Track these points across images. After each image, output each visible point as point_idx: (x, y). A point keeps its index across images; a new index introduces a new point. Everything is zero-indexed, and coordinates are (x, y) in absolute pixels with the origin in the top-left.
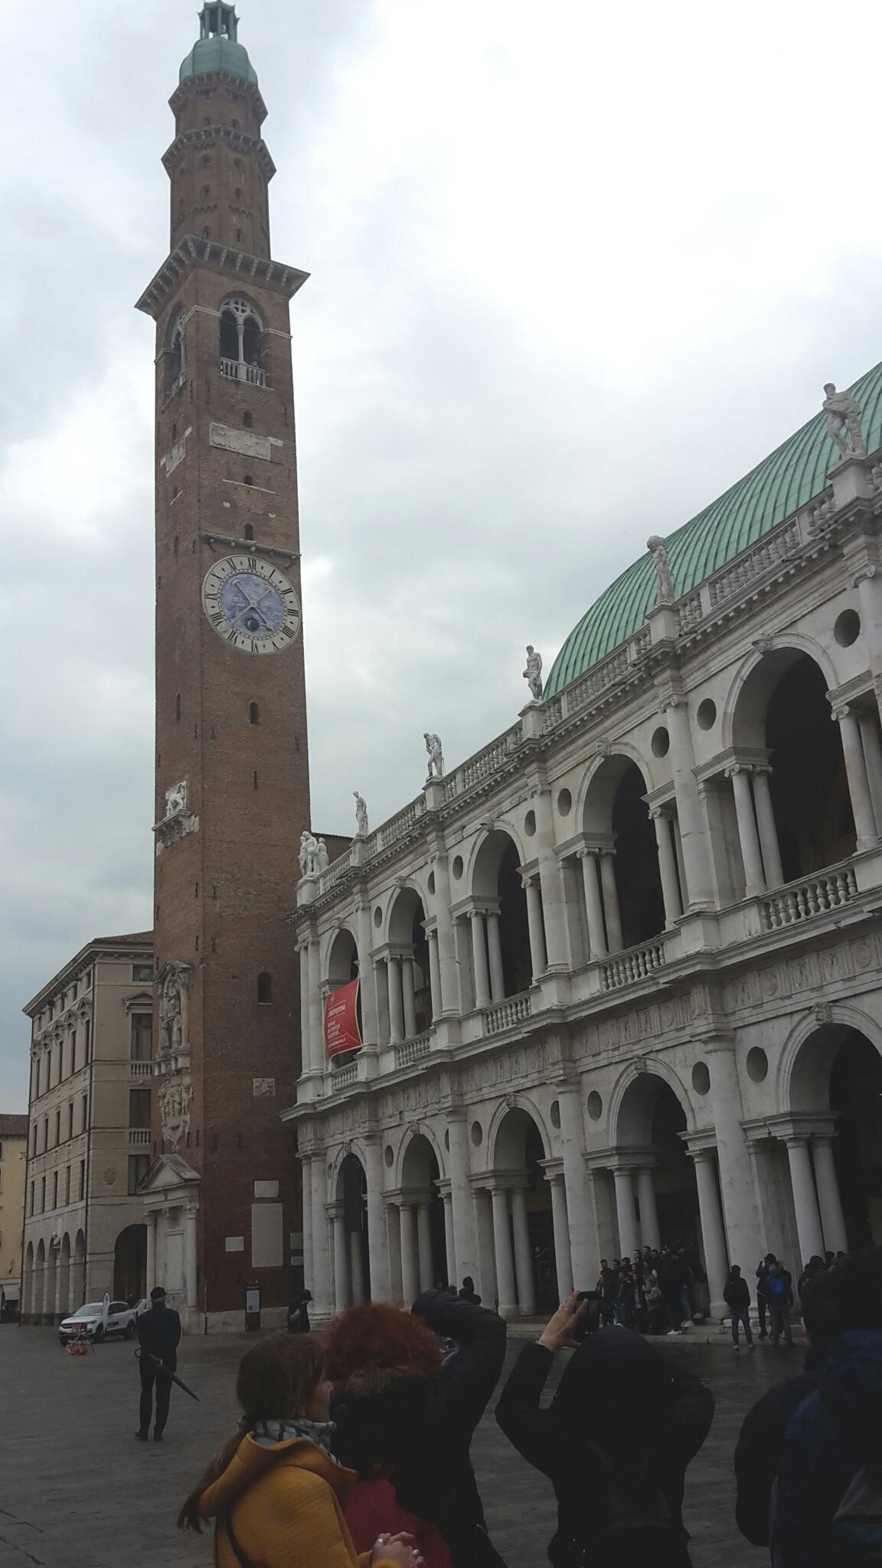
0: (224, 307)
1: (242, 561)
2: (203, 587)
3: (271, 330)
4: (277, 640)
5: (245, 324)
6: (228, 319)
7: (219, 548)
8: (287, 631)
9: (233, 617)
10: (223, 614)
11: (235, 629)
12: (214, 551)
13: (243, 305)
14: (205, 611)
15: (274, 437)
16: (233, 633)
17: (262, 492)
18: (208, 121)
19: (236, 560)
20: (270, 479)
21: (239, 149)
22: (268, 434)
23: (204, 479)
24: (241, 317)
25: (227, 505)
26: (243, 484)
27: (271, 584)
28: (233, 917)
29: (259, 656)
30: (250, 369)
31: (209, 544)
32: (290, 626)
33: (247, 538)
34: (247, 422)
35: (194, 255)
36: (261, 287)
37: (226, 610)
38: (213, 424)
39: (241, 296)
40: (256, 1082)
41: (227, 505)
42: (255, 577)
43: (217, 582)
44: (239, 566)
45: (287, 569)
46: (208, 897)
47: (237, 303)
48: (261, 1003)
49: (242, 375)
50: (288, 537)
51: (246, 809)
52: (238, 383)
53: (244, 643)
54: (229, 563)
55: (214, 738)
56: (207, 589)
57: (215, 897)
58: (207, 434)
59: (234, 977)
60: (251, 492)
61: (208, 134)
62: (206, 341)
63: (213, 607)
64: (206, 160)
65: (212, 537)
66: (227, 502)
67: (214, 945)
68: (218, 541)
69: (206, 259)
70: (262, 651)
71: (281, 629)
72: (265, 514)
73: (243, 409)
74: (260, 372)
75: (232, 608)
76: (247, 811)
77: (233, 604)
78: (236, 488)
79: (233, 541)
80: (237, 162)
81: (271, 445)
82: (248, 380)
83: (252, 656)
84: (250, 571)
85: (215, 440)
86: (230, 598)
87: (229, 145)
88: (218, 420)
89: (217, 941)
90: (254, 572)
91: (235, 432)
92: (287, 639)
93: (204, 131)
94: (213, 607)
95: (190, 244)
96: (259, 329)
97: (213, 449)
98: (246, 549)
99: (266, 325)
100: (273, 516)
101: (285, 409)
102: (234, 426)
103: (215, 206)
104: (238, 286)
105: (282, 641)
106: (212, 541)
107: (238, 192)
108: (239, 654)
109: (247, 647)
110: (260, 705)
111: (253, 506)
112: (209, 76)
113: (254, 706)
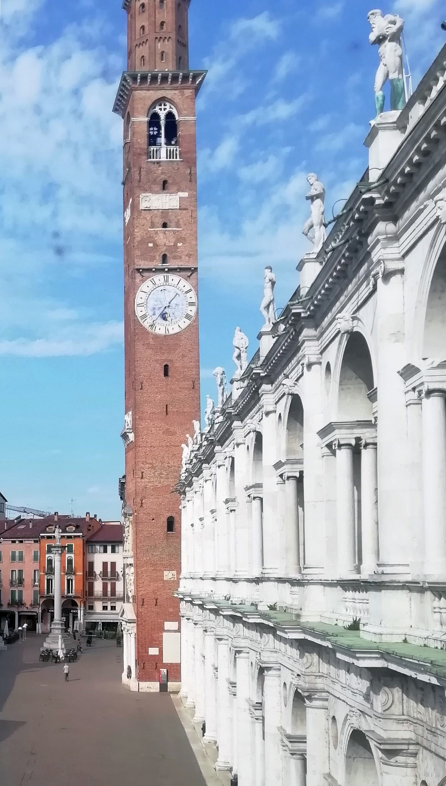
0: (152, 111)
1: (159, 278)
2: (135, 300)
7: (146, 274)
10: (147, 314)
13: (165, 105)
14: (137, 314)
15: (183, 191)
17: (174, 231)
22: (179, 190)
23: (137, 232)
24: (162, 115)
29: (171, 335)
30: (169, 149)
32: (190, 313)
34: (165, 185)
35: (131, 84)
36: (176, 90)
39: (161, 100)
40: (165, 573)
41: (151, 245)
43: (144, 295)
44: (157, 282)
45: (189, 277)
46: (138, 478)
47: (161, 105)
48: (168, 533)
51: (160, 427)
53: (161, 329)
54: (152, 282)
56: (138, 301)
57: (142, 478)
58: (139, 203)
59: (153, 519)
60: (166, 232)
65: (140, 269)
67: (142, 503)
70: (172, 332)
73: (162, 179)
76: (161, 428)
78: (156, 233)
82: (167, 158)
83: (165, 336)
84: (165, 284)
86: (151, 303)
88: (146, 191)
89: (143, 501)
96: (175, 118)
97: (143, 211)
99: (180, 114)
101: (190, 170)
102: (157, 193)
103: (147, 40)
104: (160, 94)
106: (141, 270)
108: (156, 337)
109: (162, 332)
110: (169, 365)
113: (166, 367)
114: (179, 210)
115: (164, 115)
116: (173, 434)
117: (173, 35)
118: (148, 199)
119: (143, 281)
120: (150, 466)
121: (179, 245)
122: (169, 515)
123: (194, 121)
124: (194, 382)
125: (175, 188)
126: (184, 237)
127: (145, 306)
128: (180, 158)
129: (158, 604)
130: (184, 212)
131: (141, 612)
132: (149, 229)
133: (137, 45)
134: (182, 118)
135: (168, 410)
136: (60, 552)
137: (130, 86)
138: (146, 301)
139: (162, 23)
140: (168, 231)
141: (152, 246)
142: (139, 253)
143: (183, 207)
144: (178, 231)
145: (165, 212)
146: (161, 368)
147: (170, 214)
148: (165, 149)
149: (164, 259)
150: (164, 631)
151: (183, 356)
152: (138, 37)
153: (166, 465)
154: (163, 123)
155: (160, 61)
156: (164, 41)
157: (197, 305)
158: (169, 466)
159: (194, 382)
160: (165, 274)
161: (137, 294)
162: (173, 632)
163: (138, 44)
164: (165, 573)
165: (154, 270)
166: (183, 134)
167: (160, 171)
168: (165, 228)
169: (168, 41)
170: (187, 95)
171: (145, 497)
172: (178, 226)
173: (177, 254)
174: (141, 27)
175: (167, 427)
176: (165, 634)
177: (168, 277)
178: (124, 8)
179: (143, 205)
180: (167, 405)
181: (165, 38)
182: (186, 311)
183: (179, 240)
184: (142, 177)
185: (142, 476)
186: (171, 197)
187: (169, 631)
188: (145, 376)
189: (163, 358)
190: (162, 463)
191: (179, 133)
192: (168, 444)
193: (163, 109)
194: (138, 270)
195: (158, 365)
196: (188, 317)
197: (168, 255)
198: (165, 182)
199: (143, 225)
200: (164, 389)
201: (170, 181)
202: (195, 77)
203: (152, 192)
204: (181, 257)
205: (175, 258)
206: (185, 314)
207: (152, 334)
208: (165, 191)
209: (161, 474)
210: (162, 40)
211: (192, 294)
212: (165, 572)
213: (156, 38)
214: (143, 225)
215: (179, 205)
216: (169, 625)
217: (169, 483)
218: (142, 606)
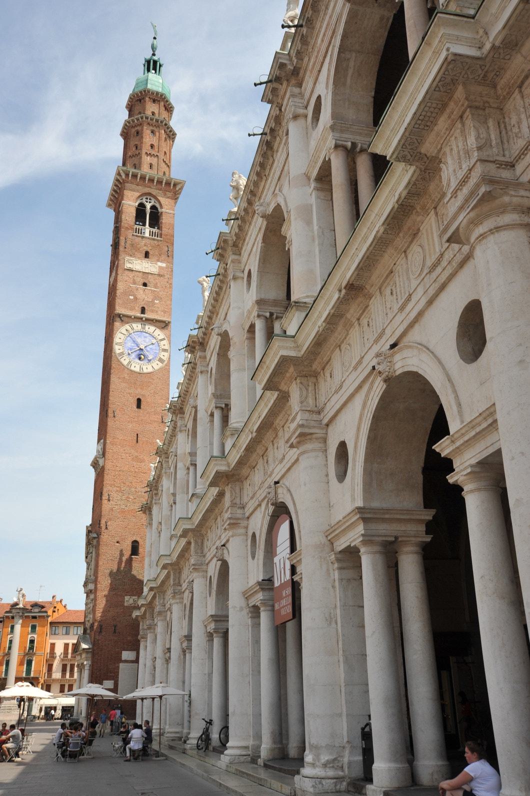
1: (137, 326)
3: (163, 210)
4: (154, 365)
5: (150, 209)
6: (142, 205)
12: (122, 321)
13: (150, 199)
15: (161, 262)
16: (130, 362)
19: (134, 325)
21: (154, 125)
22: (158, 261)
24: (148, 206)
25: (132, 297)
26: (142, 287)
27: (153, 337)
30: (151, 231)
31: (120, 317)
34: (147, 255)
36: (160, 190)
38: (127, 258)
40: (127, 598)
41: (132, 297)
42: (145, 334)
47: (147, 199)
50: (165, 312)
53: (136, 366)
61: (138, 120)
63: (119, 349)
66: (132, 296)
69: (130, 178)
70: (145, 371)
72: (153, 301)
74: (157, 232)
79: (133, 315)
82: (150, 235)
84: (142, 330)
85: (128, 265)
87: (149, 124)
90: (144, 331)
91: (139, 261)
94: (119, 349)
95: (121, 172)
100: (158, 302)
104: (147, 190)
105: (157, 365)
107: (152, 146)
109: (137, 369)
110: (142, 400)
112: (141, 92)
113: (139, 401)
121: (156, 301)
129: (117, 631)
136: (21, 614)
140: (147, 289)
143: (161, 273)
144: (156, 291)
148: (149, 230)
149: (143, 310)
150: (121, 661)
153: (133, 490)
157: (169, 351)
162: (129, 663)
164: (127, 598)
167: (143, 244)
172: (156, 288)
175: (136, 454)
176: (121, 665)
180: (137, 435)
183: (155, 298)
190: (130, 487)
196: (161, 360)
197: (146, 308)
200: (136, 420)
201: (151, 253)
205: (152, 311)
211: (165, 342)
212: (126, 597)
216: (126, 655)
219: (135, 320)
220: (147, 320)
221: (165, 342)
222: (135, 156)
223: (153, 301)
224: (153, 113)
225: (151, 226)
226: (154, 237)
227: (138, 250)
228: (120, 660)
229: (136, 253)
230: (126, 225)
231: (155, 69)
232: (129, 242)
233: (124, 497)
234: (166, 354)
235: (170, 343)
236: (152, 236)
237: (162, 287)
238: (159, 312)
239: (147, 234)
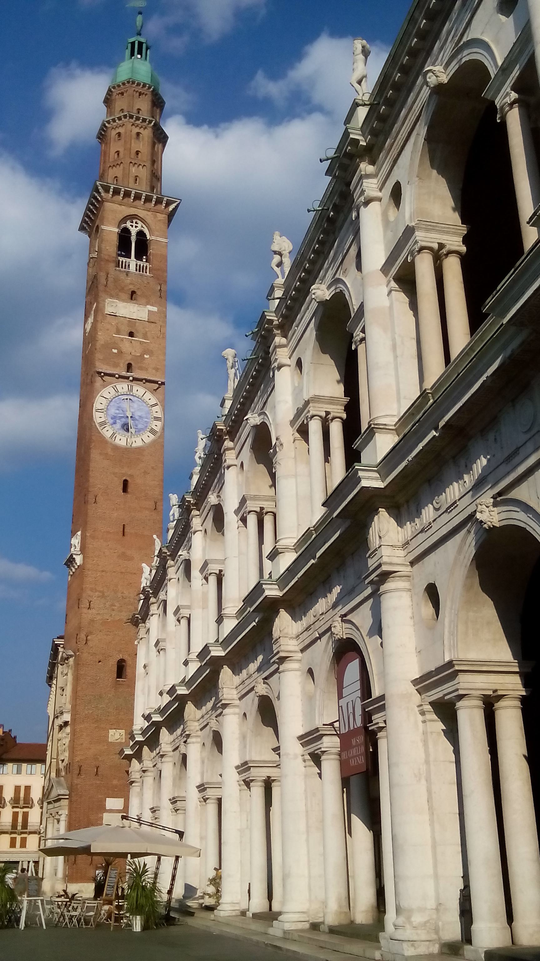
0: (123, 225)
1: (123, 387)
2: (94, 405)
7: (106, 378)
8: (153, 431)
9: (115, 423)
10: (107, 421)
11: (115, 431)
13: (136, 223)
15: (152, 305)
16: (114, 434)
17: (141, 341)
18: (122, 110)
19: (119, 387)
20: (146, 333)
22: (148, 303)
24: (134, 231)
25: (115, 351)
28: (101, 621)
30: (138, 264)
31: (102, 377)
32: (154, 427)
33: (128, 372)
36: (149, 211)
37: (110, 419)
38: (108, 300)
40: (111, 732)
41: (115, 351)
47: (132, 222)
48: (118, 679)
49: (133, 268)
50: (157, 369)
52: (127, 274)
53: (121, 440)
54: (114, 389)
55: (95, 502)
58: (104, 307)
59: (100, 662)
62: (108, 248)
64: (119, 134)
65: (102, 372)
66: (115, 349)
67: (87, 640)
68: (106, 374)
71: (148, 430)
72: (142, 356)
75: (114, 418)
77: (115, 415)
78: (122, 340)
79: (117, 374)
80: (138, 134)
81: (149, 311)
82: (136, 270)
84: (128, 393)
85: (109, 309)
86: (113, 411)
88: (112, 296)
90: (131, 394)
92: (152, 437)
93: (117, 118)
96: (147, 238)
98: (127, 378)
101: (161, 287)
102: (124, 301)
103: (122, 163)
104: (132, 211)
105: (148, 438)
106: (102, 374)
108: (116, 448)
111: (133, 351)
114: (147, 323)
115: (135, 231)
116: (131, 559)
117: (148, 164)
118: (114, 305)
119: (105, 387)
120: (100, 594)
121: (146, 356)
122: (121, 657)
123: (166, 244)
124: (156, 503)
125: (144, 301)
126: (151, 350)
127: (105, 412)
128: (149, 273)
130: (153, 325)
131: (77, 785)
132: (114, 335)
133: (110, 166)
134: (153, 238)
135: (125, 530)
137: (101, 197)
138: (106, 407)
139: (137, 153)
140: (134, 340)
141: (116, 352)
142: (101, 357)
144: (145, 343)
145: (132, 321)
146: (120, 482)
147: (137, 324)
148: (135, 263)
151: (145, 473)
152: (111, 160)
154: (133, 239)
155: (133, 183)
156: (138, 166)
158: (123, 597)
159: (156, 503)
160: (130, 383)
161: (97, 399)
163: (112, 165)
165: (117, 376)
166: (154, 252)
168: (132, 337)
169: (142, 168)
170: (159, 219)
171: (91, 633)
172: (145, 337)
173: (144, 366)
174: (116, 152)
177: (132, 386)
178: (99, 138)
179: (109, 309)
180: (124, 525)
181: (140, 165)
182: (151, 425)
183: (145, 352)
184: (108, 282)
185: (90, 605)
186: (139, 308)
187: (111, 811)
188: (100, 489)
189: (123, 472)
191: (151, 251)
192: (123, 571)
193: (134, 226)
194: (99, 373)
195: (116, 479)
198: (133, 293)
199: (108, 330)
201: (139, 293)
202: (168, 203)
203: (118, 298)
204: (147, 370)
205: (141, 368)
206: (150, 428)
207: (111, 444)
208: (132, 301)
209: (113, 605)
210: (136, 166)
212: (110, 731)
213: (131, 162)
214: (108, 330)
215: (147, 318)
216: (114, 803)
217: (122, 617)
218: (78, 775)
219: (120, 379)
220: (135, 379)
221: (157, 408)
222: (116, 167)
223: (142, 356)
224: (139, 110)
225: (139, 257)
226: (141, 273)
227: (122, 290)
228: (102, 808)
229: (120, 294)
230: (106, 257)
231: (140, 52)
232: (111, 279)
233: (108, 604)
234: (159, 424)
235: (164, 410)
236: (140, 271)
237: (153, 338)
238: (150, 370)
239: (133, 268)
